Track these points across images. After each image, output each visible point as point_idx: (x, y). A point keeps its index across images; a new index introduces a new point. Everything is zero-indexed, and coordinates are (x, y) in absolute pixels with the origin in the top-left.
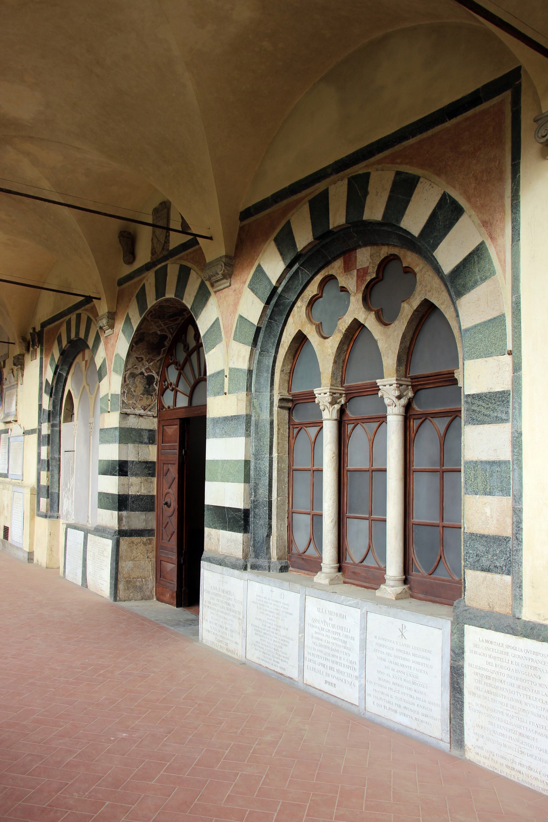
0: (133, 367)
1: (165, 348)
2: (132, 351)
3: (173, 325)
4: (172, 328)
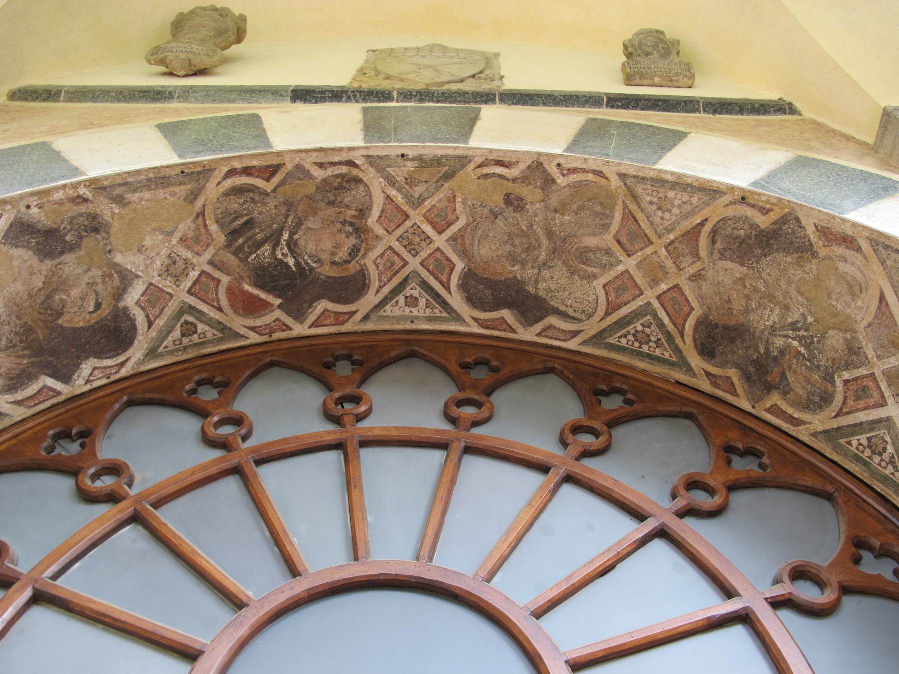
1: (58, 385)
3: (210, 322)
4: (189, 330)
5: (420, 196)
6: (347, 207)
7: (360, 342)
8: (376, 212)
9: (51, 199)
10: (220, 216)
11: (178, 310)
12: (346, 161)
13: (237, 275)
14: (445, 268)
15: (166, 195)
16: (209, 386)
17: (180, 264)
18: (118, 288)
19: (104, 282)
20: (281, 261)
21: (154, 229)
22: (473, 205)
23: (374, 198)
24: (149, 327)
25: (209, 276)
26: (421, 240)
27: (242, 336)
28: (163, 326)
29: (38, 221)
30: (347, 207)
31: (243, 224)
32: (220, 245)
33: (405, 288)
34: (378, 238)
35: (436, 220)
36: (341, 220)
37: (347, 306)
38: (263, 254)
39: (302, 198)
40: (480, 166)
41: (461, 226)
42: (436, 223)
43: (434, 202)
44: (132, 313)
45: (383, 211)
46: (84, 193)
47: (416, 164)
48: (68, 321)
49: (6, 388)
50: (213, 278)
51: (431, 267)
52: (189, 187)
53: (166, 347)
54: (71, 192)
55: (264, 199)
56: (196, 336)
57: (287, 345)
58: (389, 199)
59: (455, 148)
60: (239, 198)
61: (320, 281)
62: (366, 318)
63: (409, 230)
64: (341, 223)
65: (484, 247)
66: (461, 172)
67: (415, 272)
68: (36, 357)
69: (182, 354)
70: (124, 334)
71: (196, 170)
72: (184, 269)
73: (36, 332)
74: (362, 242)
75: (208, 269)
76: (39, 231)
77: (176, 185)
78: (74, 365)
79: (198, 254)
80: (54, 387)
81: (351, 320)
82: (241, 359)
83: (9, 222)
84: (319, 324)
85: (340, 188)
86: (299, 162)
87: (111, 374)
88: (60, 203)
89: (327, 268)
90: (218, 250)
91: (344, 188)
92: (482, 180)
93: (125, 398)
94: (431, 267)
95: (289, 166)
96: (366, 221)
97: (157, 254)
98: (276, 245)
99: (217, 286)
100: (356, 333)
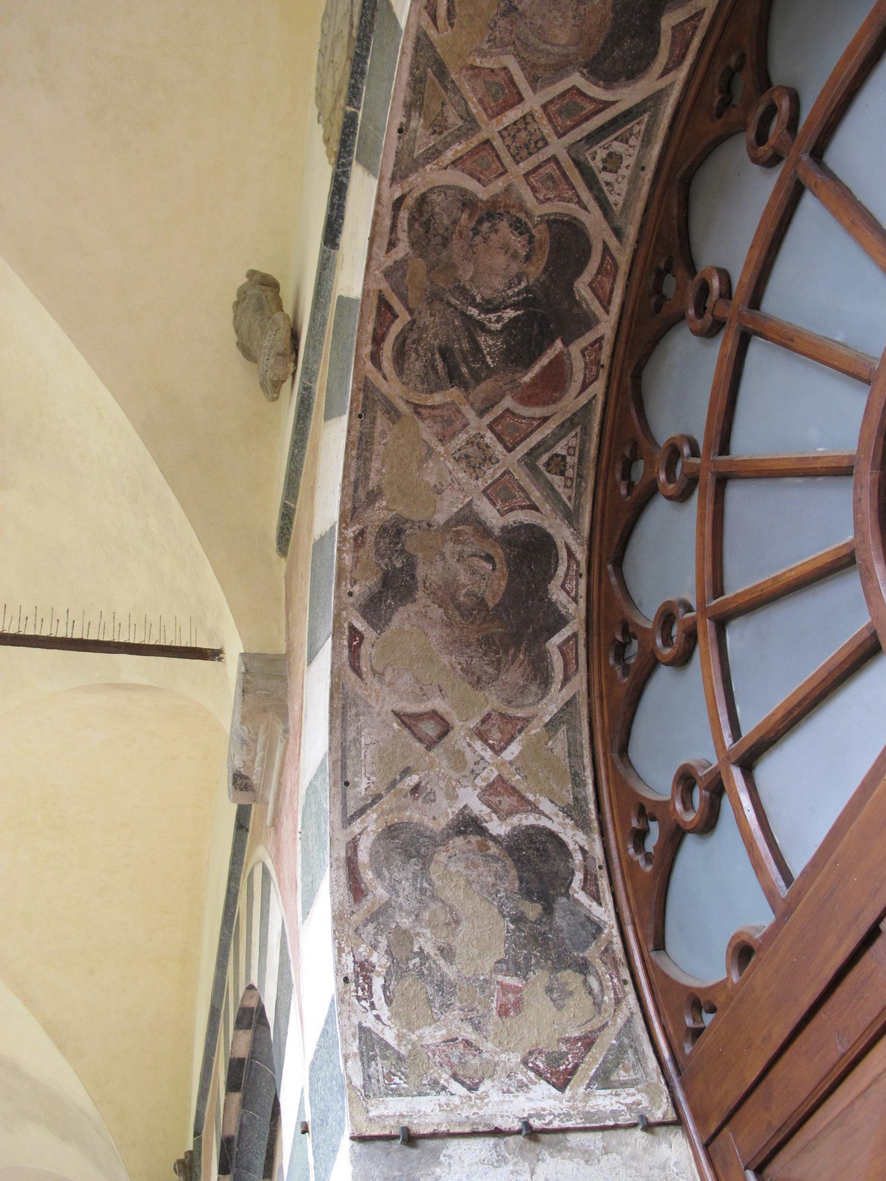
0: (393, 784)
2: (357, 670)
3: (557, 436)
4: (558, 464)
5: (462, 118)
6: (455, 222)
7: (648, 252)
8: (472, 185)
9: (349, 568)
10: (426, 386)
11: (527, 470)
12: (393, 210)
13: (507, 387)
14: (575, 103)
15: (382, 443)
16: (633, 466)
17: (470, 450)
18: (476, 529)
19: (463, 543)
20: (505, 326)
21: (419, 468)
22: (489, 41)
23: (451, 183)
24: (537, 509)
25: (496, 421)
26: (526, 129)
27: (590, 402)
28: (542, 494)
29: (370, 590)
30: (455, 222)
31: (443, 361)
32: (462, 396)
33: (591, 168)
34: (508, 190)
35: (501, 101)
36: (471, 234)
37: (593, 254)
38: (490, 346)
39: (429, 279)
40: (434, 19)
41: (517, 65)
42: (505, 101)
43: (475, 99)
44: (511, 523)
45: (471, 175)
46: (354, 532)
47: (415, 114)
48: (494, 597)
49: (543, 686)
50: (502, 416)
51: (569, 123)
52: (379, 414)
53: (569, 498)
54: (348, 545)
55: (419, 328)
56: (568, 459)
57: (621, 347)
58: (457, 163)
59: (403, 53)
60: (409, 359)
61: (547, 283)
62: (618, 233)
63: (507, 143)
64: (475, 235)
65: (556, 36)
66: (439, 50)
67: (570, 148)
68: (522, 643)
69: (586, 482)
70: (533, 540)
71: (361, 399)
72: (479, 448)
73: (493, 634)
74: (508, 212)
75: (488, 419)
76: (380, 592)
77: (372, 428)
78: (548, 608)
79: (465, 426)
80: (566, 636)
81: (616, 254)
82: (618, 412)
83: (361, 618)
84: (606, 299)
85: (427, 225)
86: (382, 272)
87: (577, 572)
88: (356, 560)
89: (532, 269)
90: (468, 400)
91: (429, 220)
92: (456, 21)
93: (610, 567)
94: (569, 123)
95: (384, 285)
96: (481, 201)
97: (450, 473)
98: (482, 327)
99: (513, 414)
100: (635, 252)
